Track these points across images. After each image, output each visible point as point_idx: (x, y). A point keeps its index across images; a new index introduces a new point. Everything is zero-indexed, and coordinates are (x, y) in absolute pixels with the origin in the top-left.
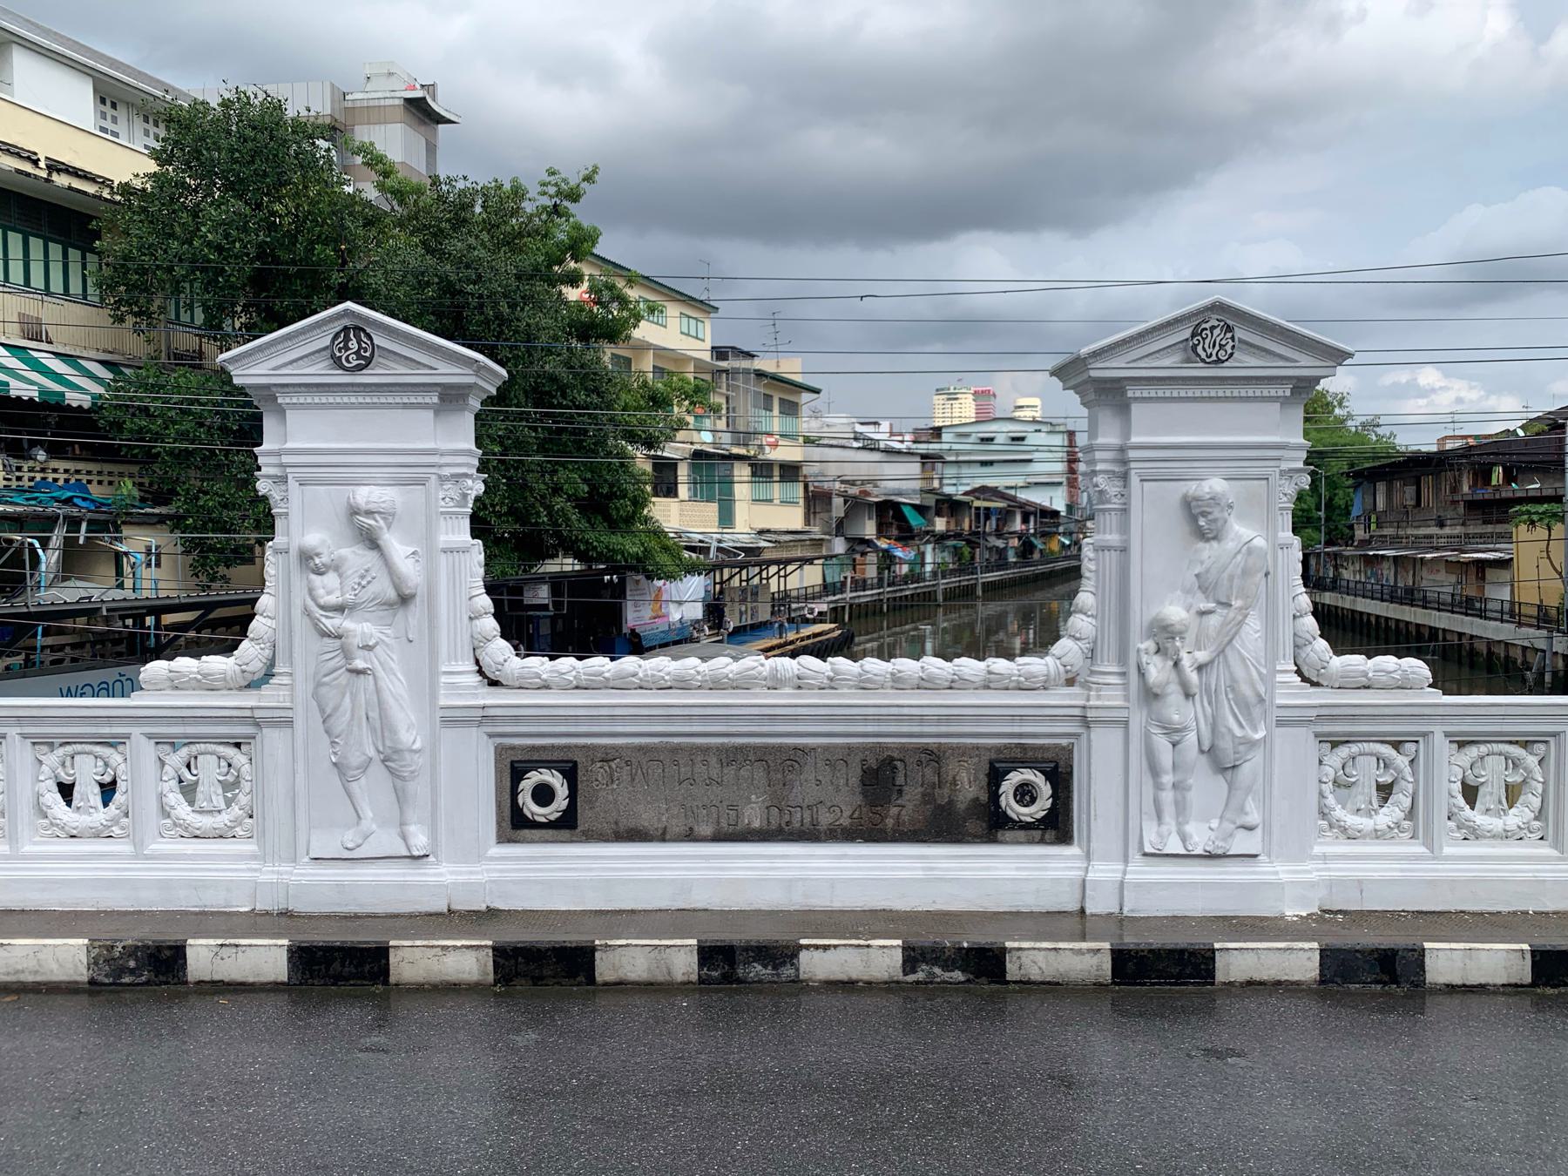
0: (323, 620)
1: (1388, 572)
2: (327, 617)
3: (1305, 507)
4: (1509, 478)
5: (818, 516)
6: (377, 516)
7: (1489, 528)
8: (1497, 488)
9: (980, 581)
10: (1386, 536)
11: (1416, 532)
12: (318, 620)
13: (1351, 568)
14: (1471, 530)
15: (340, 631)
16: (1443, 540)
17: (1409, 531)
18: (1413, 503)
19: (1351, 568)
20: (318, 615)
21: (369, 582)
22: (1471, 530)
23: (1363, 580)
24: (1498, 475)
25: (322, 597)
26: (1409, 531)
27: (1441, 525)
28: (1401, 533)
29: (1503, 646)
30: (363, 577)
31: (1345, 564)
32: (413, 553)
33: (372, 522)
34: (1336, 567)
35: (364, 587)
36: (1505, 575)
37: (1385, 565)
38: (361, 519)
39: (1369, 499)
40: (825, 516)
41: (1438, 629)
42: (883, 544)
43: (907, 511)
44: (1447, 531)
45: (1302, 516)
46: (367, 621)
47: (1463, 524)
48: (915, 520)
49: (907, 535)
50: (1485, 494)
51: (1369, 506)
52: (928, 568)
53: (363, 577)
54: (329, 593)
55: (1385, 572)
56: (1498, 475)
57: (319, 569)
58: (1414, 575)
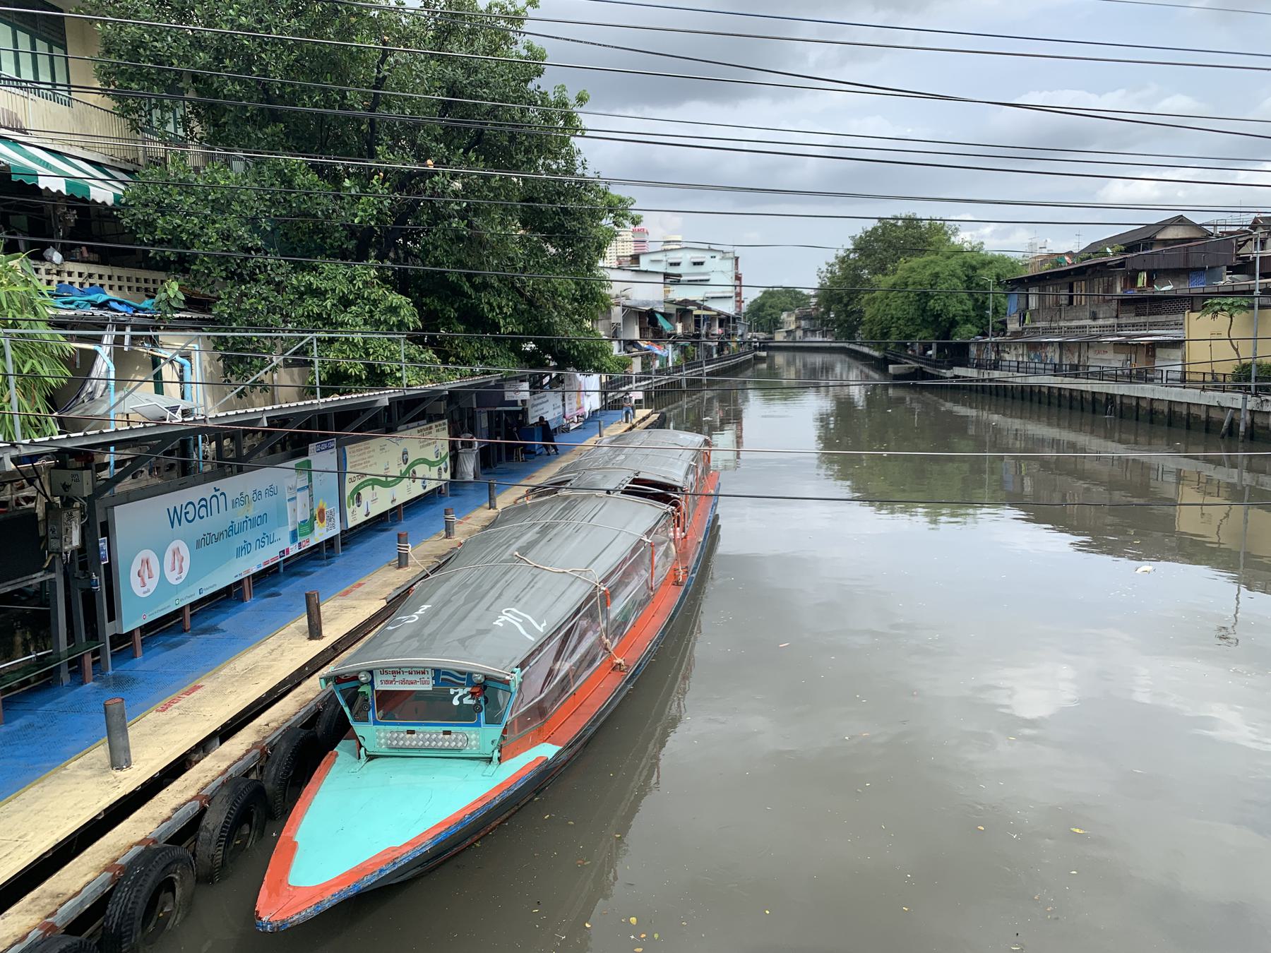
1: (1053, 355)
3: (965, 308)
4: (1150, 282)
5: (599, 322)
7: (1142, 319)
8: (1141, 290)
9: (705, 371)
10: (1038, 328)
11: (1068, 324)
13: (1013, 352)
14: (1123, 321)
16: (1095, 329)
17: (1062, 324)
18: (1066, 302)
19: (1013, 352)
22: (1123, 321)
23: (1025, 360)
24: (1142, 279)
26: (1062, 324)
27: (1095, 318)
28: (1053, 325)
29: (1185, 406)
31: (1007, 350)
34: (998, 352)
36: (1176, 354)
37: (1050, 349)
39: (1023, 301)
40: (606, 322)
41: (1115, 395)
42: (644, 344)
43: (658, 316)
44: (1100, 322)
45: (963, 316)
47: (1117, 317)
48: (662, 322)
49: (659, 336)
50: (1133, 293)
51: (1023, 306)
52: (670, 364)
55: (1049, 355)
56: (1142, 279)
58: (1079, 356)
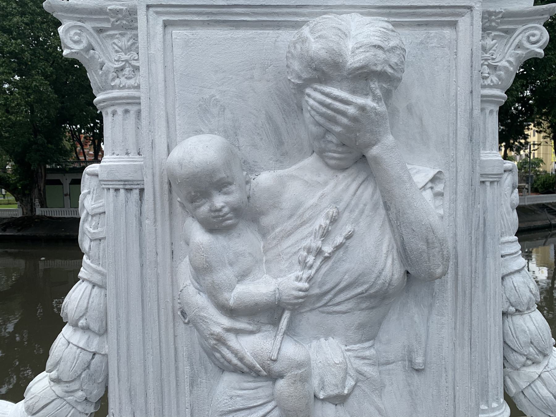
0: (233, 341)
2: (238, 332)
6: (374, 85)
12: (221, 340)
15: (277, 367)
20: (217, 330)
21: (338, 248)
25: (231, 288)
30: (325, 235)
32: (434, 180)
33: (368, 102)
35: (327, 259)
38: (336, 92)
46: (329, 333)
53: (325, 235)
54: (242, 276)
57: (224, 218)
